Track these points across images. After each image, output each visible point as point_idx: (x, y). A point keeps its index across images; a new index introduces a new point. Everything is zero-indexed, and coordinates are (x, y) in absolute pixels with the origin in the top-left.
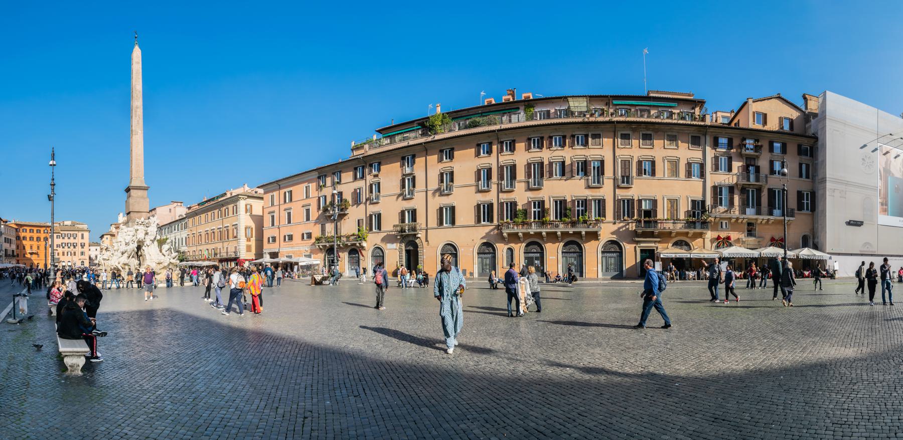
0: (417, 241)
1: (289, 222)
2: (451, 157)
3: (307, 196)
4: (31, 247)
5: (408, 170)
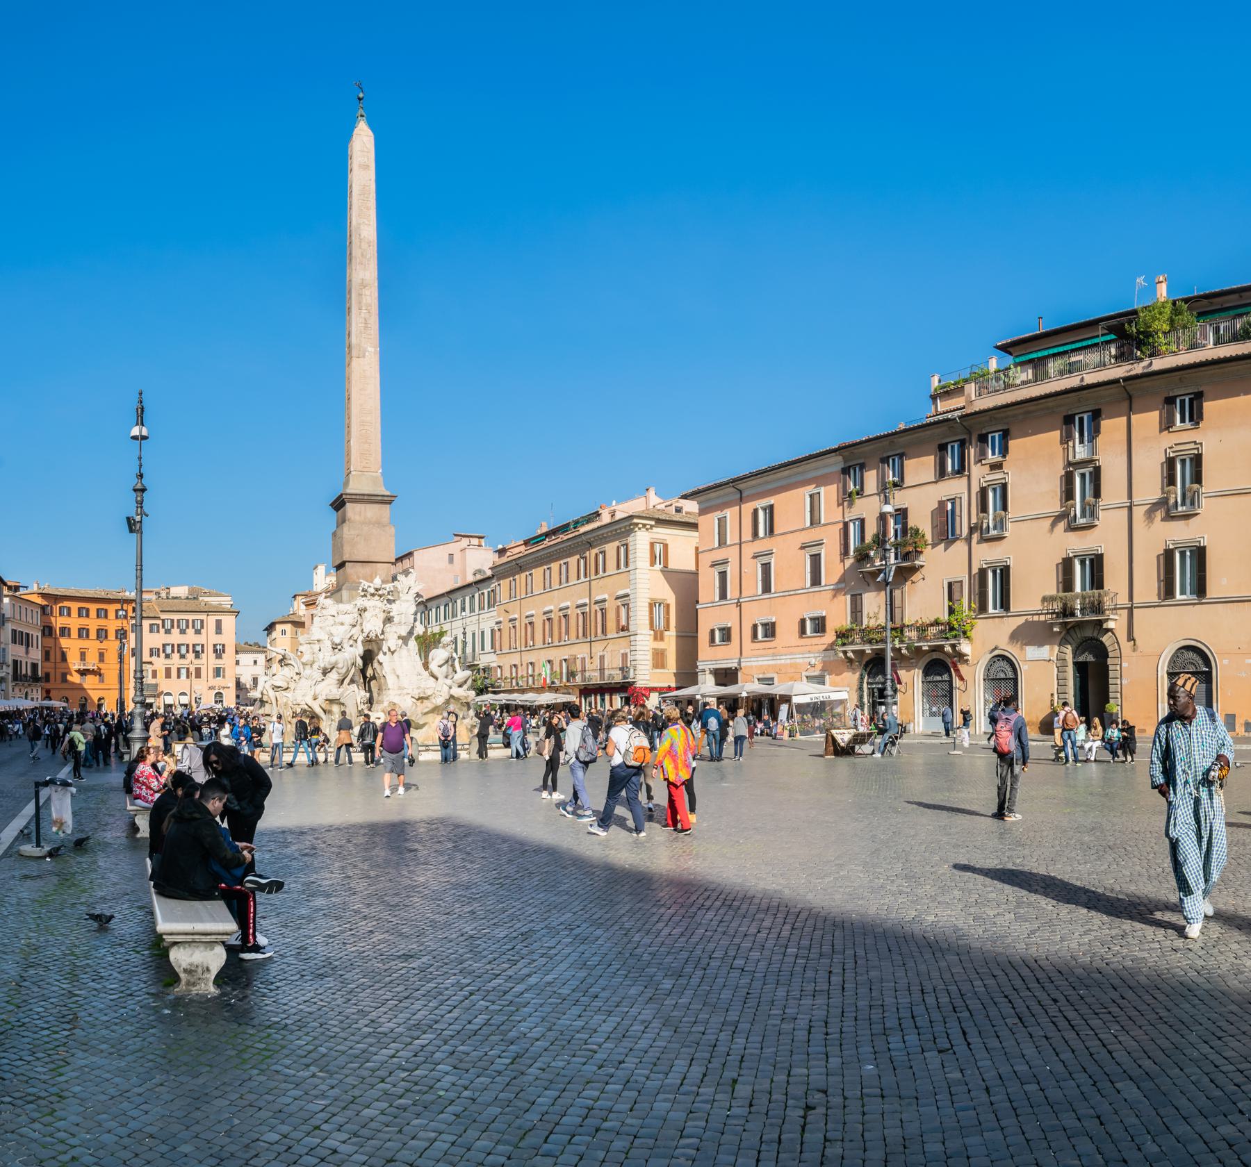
0: (1106, 639)
1: (767, 588)
2: (1195, 416)
3: (813, 519)
4: (83, 656)
5: (1081, 452)
